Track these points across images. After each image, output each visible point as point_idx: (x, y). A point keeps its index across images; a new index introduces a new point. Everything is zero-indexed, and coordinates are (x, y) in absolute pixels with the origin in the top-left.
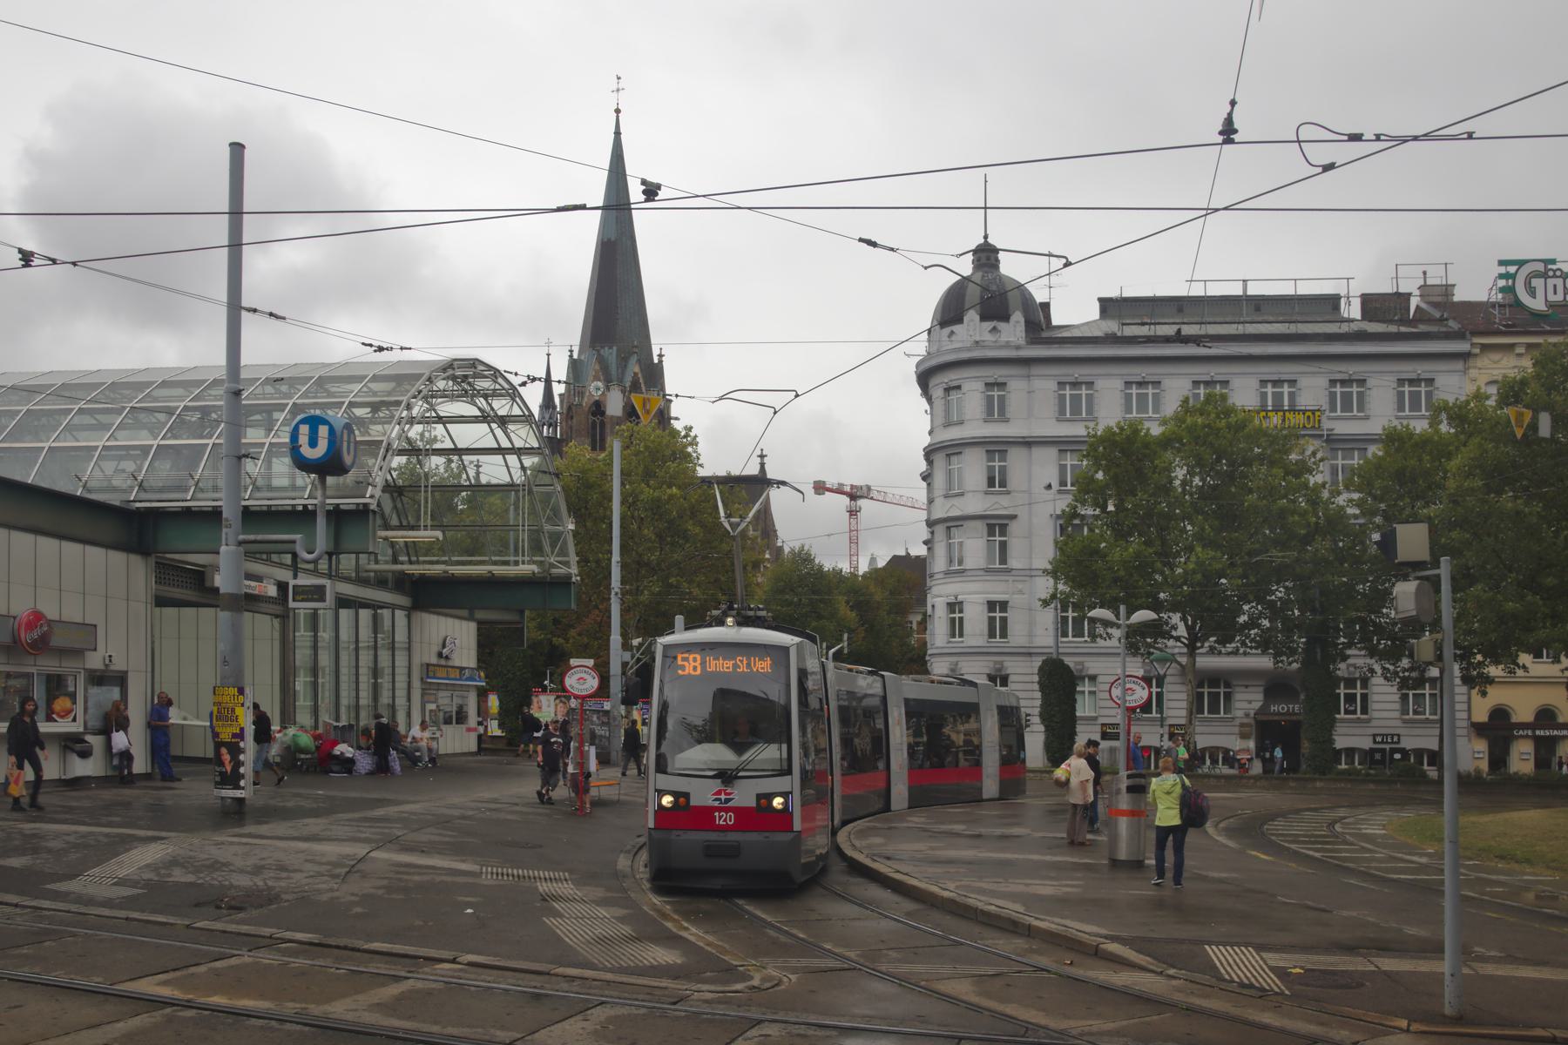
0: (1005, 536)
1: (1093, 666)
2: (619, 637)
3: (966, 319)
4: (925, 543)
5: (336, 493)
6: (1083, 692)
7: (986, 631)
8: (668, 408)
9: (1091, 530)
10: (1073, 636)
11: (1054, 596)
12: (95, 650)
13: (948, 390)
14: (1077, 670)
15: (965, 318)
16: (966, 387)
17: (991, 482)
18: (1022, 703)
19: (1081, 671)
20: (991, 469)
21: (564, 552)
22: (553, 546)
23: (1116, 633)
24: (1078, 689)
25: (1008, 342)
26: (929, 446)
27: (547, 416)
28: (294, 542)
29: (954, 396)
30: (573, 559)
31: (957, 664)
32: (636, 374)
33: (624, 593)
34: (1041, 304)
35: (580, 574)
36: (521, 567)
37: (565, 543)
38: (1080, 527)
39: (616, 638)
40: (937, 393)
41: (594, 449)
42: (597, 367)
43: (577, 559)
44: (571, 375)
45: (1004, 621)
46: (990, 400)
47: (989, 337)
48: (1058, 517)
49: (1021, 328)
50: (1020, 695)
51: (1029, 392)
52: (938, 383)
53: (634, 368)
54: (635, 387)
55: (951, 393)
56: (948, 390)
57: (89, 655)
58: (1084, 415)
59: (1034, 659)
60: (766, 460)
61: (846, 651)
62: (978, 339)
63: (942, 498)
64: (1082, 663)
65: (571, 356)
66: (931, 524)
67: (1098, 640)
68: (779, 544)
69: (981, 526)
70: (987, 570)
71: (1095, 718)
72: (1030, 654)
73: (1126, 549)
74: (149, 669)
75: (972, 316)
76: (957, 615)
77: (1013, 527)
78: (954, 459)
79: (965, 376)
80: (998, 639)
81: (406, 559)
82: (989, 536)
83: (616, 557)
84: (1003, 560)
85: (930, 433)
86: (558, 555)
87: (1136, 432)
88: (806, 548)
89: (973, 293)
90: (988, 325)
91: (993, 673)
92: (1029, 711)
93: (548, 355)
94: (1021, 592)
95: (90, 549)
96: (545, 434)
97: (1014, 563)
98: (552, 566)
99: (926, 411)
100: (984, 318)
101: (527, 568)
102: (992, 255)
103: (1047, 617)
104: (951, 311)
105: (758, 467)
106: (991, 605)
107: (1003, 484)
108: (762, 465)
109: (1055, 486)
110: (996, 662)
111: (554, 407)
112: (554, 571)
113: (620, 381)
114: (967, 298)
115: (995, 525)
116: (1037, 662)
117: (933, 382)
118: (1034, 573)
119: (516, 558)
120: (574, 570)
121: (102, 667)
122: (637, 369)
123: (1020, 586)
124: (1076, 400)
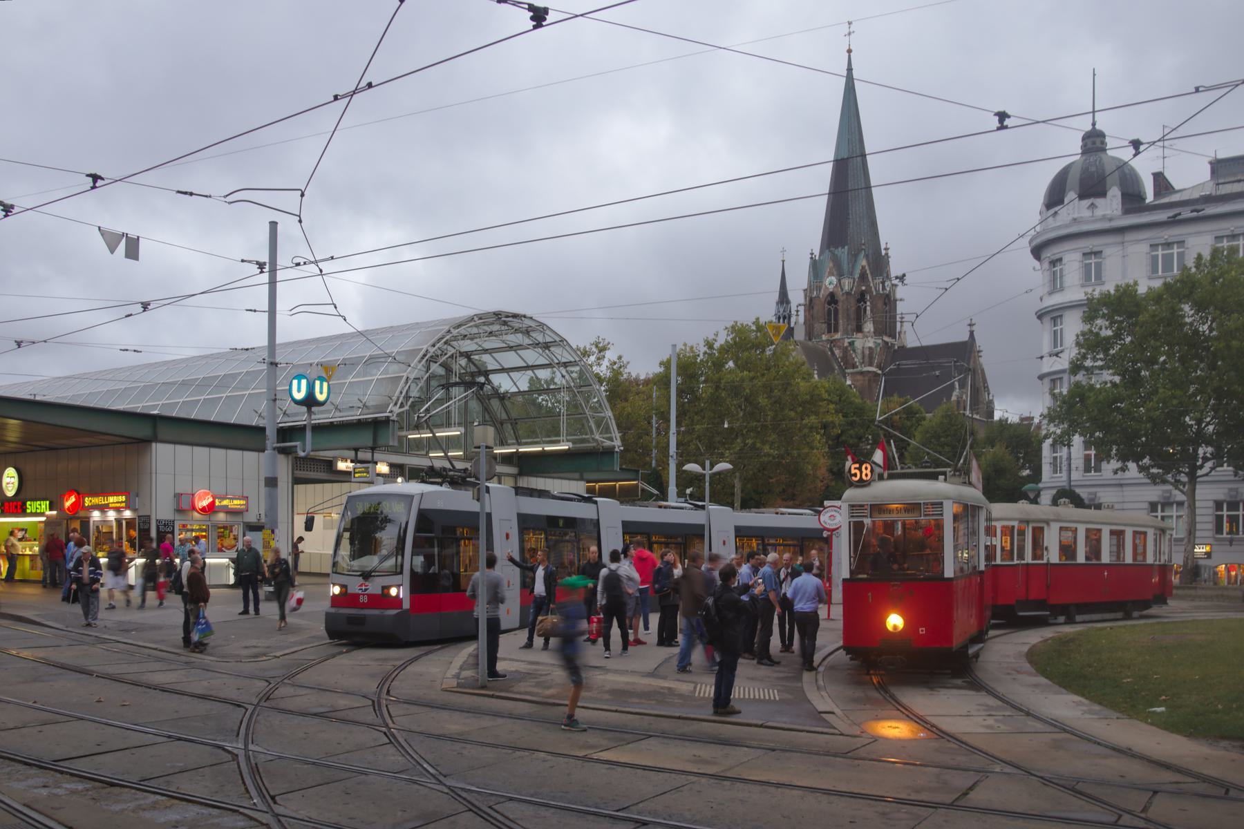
2: (675, 488)
5: (320, 417)
6: (1171, 517)
12: (247, 511)
13: (1054, 263)
19: (1169, 498)
22: (598, 426)
27: (782, 310)
28: (296, 446)
29: (1058, 268)
37: (607, 423)
40: (1046, 265)
41: (829, 331)
44: (812, 274)
46: (1088, 267)
47: (1087, 214)
52: (1049, 254)
54: (863, 277)
56: (1054, 263)
57: (245, 513)
62: (1076, 216)
79: (1066, 249)
81: (514, 441)
86: (601, 433)
90: (1086, 202)
93: (783, 261)
100: (1082, 196)
102: (1098, 140)
104: (1055, 198)
113: (851, 274)
117: (1043, 256)
121: (256, 521)
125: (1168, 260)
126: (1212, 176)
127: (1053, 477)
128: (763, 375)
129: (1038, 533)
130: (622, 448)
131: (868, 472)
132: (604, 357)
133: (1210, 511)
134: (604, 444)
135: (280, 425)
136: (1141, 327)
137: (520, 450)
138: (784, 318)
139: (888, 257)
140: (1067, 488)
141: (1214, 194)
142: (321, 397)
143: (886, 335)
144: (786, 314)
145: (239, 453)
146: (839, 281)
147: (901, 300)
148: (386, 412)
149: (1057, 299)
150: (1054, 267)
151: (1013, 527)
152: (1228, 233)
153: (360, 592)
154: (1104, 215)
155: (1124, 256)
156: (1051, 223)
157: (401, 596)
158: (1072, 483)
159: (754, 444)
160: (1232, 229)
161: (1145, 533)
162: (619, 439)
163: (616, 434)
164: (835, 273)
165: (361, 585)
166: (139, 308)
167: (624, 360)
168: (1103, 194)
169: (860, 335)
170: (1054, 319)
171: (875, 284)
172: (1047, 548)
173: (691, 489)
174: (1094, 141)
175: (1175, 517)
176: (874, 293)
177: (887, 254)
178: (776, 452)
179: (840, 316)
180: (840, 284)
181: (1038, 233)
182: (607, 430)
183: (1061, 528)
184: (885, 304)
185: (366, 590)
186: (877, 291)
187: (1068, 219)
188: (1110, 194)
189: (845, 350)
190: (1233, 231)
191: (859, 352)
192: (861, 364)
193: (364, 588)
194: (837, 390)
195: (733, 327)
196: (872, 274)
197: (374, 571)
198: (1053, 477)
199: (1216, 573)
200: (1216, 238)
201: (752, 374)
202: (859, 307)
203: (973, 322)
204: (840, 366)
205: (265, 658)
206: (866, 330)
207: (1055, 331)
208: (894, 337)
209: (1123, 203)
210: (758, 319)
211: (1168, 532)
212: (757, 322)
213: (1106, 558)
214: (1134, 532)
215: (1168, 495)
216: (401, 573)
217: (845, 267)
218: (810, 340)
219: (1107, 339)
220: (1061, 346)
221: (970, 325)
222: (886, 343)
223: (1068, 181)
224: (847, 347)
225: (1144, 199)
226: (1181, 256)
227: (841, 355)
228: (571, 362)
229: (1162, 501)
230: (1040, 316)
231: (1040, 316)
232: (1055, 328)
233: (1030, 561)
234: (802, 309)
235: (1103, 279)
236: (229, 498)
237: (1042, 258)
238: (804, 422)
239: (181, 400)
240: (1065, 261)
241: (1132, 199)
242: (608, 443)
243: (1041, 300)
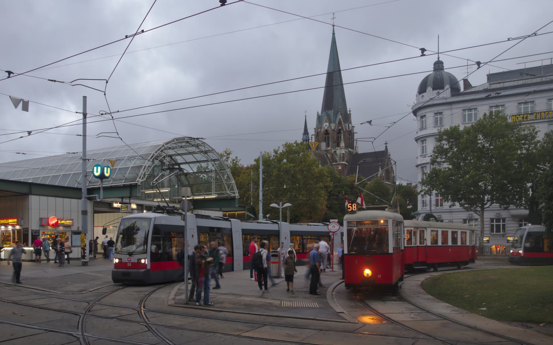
2: (262, 214)
3: (427, 90)
5: (106, 184)
13: (422, 117)
15: (427, 90)
16: (428, 115)
19: (471, 217)
22: (228, 188)
27: (305, 137)
28: (96, 197)
32: (340, 119)
33: (264, 200)
37: (232, 186)
40: (419, 118)
42: (326, 118)
44: (318, 122)
51: (452, 115)
54: (340, 123)
56: (422, 117)
60: (387, 145)
63: (420, 157)
74: (92, 230)
79: (427, 111)
86: (229, 191)
90: (436, 92)
93: (306, 116)
95: (72, 200)
100: (434, 89)
102: (440, 65)
104: (422, 89)
108: (386, 147)
113: (335, 122)
117: (418, 114)
122: (340, 117)
125: (470, 116)
126: (488, 81)
127: (422, 209)
128: (299, 165)
129: (422, 232)
130: (239, 197)
131: (355, 207)
132: (229, 157)
133: (489, 223)
134: (231, 195)
135: (88, 187)
136: (462, 144)
137: (194, 198)
139: (351, 115)
140: (430, 213)
141: (489, 88)
142: (107, 175)
143: (350, 148)
144: (306, 139)
145: (69, 200)
146: (330, 124)
147: (356, 133)
148: (136, 181)
149: (424, 133)
150: (422, 119)
151: (411, 230)
152: (495, 105)
153: (128, 261)
154: (443, 97)
155: (452, 115)
156: (421, 100)
157: (146, 263)
158: (432, 211)
159: (295, 195)
160: (497, 103)
161: (466, 232)
162: (237, 193)
163: (236, 191)
164: (328, 121)
165: (128, 259)
166: (27, 134)
167: (238, 158)
168: (442, 88)
169: (339, 148)
170: (422, 141)
171: (345, 126)
172: (425, 239)
173: (269, 215)
174: (438, 65)
175: (474, 225)
176: (345, 130)
177: (350, 113)
178: (305, 199)
179: (330, 140)
180: (330, 126)
181: (415, 104)
182: (232, 189)
183: (432, 231)
184: (349, 135)
185: (130, 260)
186: (346, 129)
187: (428, 99)
188: (446, 88)
189: (332, 155)
190: (497, 104)
191: (338, 155)
192: (339, 160)
193: (129, 260)
194: (330, 172)
195: (286, 144)
197: (134, 252)
198: (422, 209)
199: (491, 249)
201: (294, 165)
202: (338, 136)
203: (387, 142)
204: (330, 162)
205: (85, 292)
206: (341, 146)
207: (423, 146)
208: (353, 149)
209: (451, 92)
210: (296, 141)
211: (475, 232)
212: (296, 143)
213: (450, 243)
214: (461, 232)
215: (471, 216)
216: (146, 253)
217: (332, 118)
218: (317, 150)
219: (447, 149)
220: (425, 153)
221: (386, 144)
222: (350, 151)
223: (428, 82)
224: (333, 153)
225: (460, 90)
226: (475, 114)
227: (331, 156)
228: (216, 159)
229: (468, 219)
230: (417, 140)
231: (417, 140)
232: (423, 145)
233: (419, 245)
234: (313, 137)
235: (443, 124)
236: (64, 220)
237: (417, 115)
238: (317, 185)
239: (62, 174)
240: (427, 116)
241: (455, 90)
242: (233, 195)
243: (417, 133)
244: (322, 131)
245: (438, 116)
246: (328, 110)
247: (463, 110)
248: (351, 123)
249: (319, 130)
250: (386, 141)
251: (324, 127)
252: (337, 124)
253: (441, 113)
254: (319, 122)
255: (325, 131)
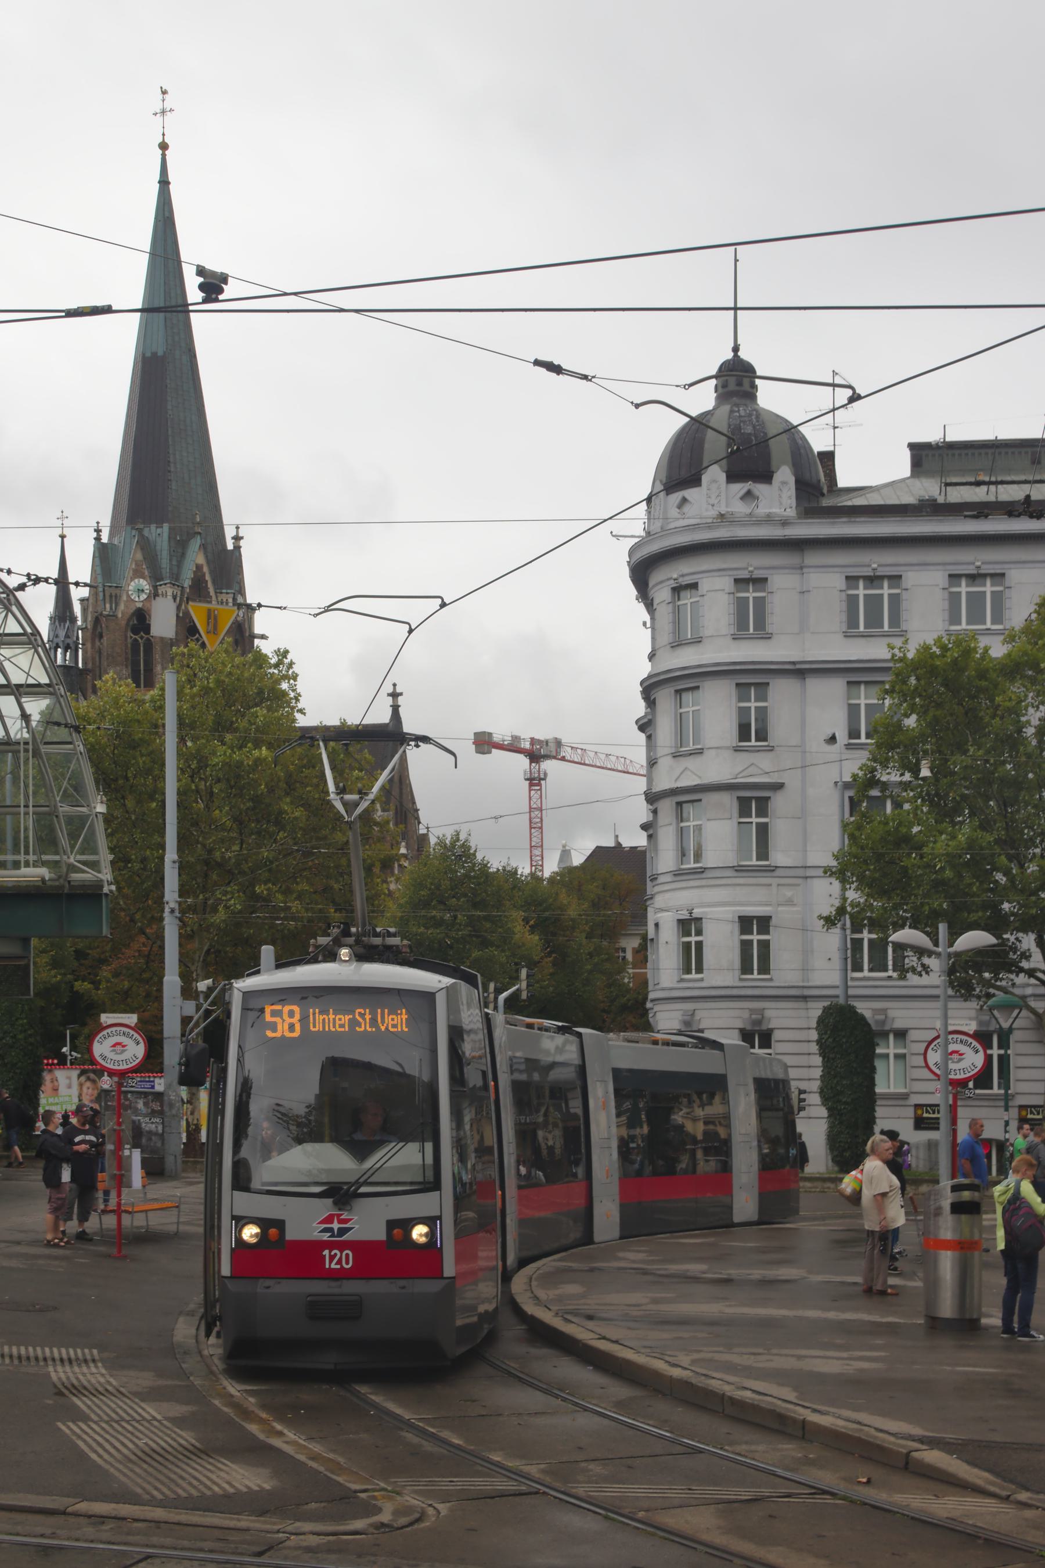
0: (766, 816)
1: (901, 1016)
4: (645, 827)
6: (886, 1056)
7: (737, 964)
8: (250, 621)
9: (898, 805)
10: (871, 970)
11: (841, 911)
13: (677, 590)
14: (877, 1022)
15: (703, 477)
16: (705, 585)
17: (744, 733)
18: (793, 1073)
19: (883, 1022)
20: (743, 712)
21: (89, 847)
22: (73, 836)
23: (933, 962)
24: (878, 1051)
25: (769, 515)
26: (650, 677)
27: (62, 634)
29: (687, 599)
30: (105, 857)
31: (693, 1015)
32: (199, 567)
34: (820, 453)
35: (116, 882)
36: (24, 870)
38: (880, 801)
39: (172, 980)
40: (662, 595)
42: (139, 556)
43: (111, 857)
44: (99, 570)
45: (765, 946)
47: (740, 508)
48: (847, 786)
49: (789, 494)
50: (789, 1060)
53: (196, 557)
55: (683, 594)
56: (677, 590)
58: (886, 628)
59: (811, 1005)
60: (401, 700)
61: (524, 996)
62: (723, 510)
63: (669, 758)
64: (884, 1011)
65: (98, 539)
66: (652, 798)
67: (909, 975)
68: (422, 831)
69: (728, 801)
70: (739, 869)
71: (905, 1097)
72: (805, 998)
73: (953, 837)
75: (714, 475)
76: (693, 939)
77: (779, 802)
78: (688, 697)
80: (755, 975)
82: (741, 816)
83: (171, 855)
84: (763, 852)
85: (652, 657)
87: (968, 652)
88: (462, 837)
89: (715, 445)
91: (749, 1027)
92: (803, 1086)
93: (63, 537)
94: (790, 902)
96: (59, 661)
97: (779, 857)
98: (72, 868)
99: (645, 624)
101: (32, 873)
103: (831, 942)
105: (390, 711)
106: (745, 923)
107: (762, 736)
108: (395, 708)
109: (842, 737)
110: (752, 1011)
111: (73, 620)
112: (76, 876)
113: (176, 579)
114: (707, 446)
115: (750, 799)
116: (816, 1010)
118: (810, 873)
119: (16, 858)
120: (106, 875)
122: (201, 560)
123: (788, 893)
124: (874, 604)
138: (66, 648)
144: (68, 641)
149: (688, 658)
156: (677, 519)
160: (978, 564)
170: (679, 692)
190: (978, 567)
196: (214, 582)
200: (950, 576)
203: (398, 690)
215: (882, 1017)
217: (165, 562)
244: (120, 615)
245: (748, 591)
246: (147, 522)
247: (847, 578)
248: (241, 591)
249: (108, 606)
250: (395, 685)
251: (128, 596)
252: (188, 590)
253: (760, 582)
254: (103, 569)
255: (133, 614)
